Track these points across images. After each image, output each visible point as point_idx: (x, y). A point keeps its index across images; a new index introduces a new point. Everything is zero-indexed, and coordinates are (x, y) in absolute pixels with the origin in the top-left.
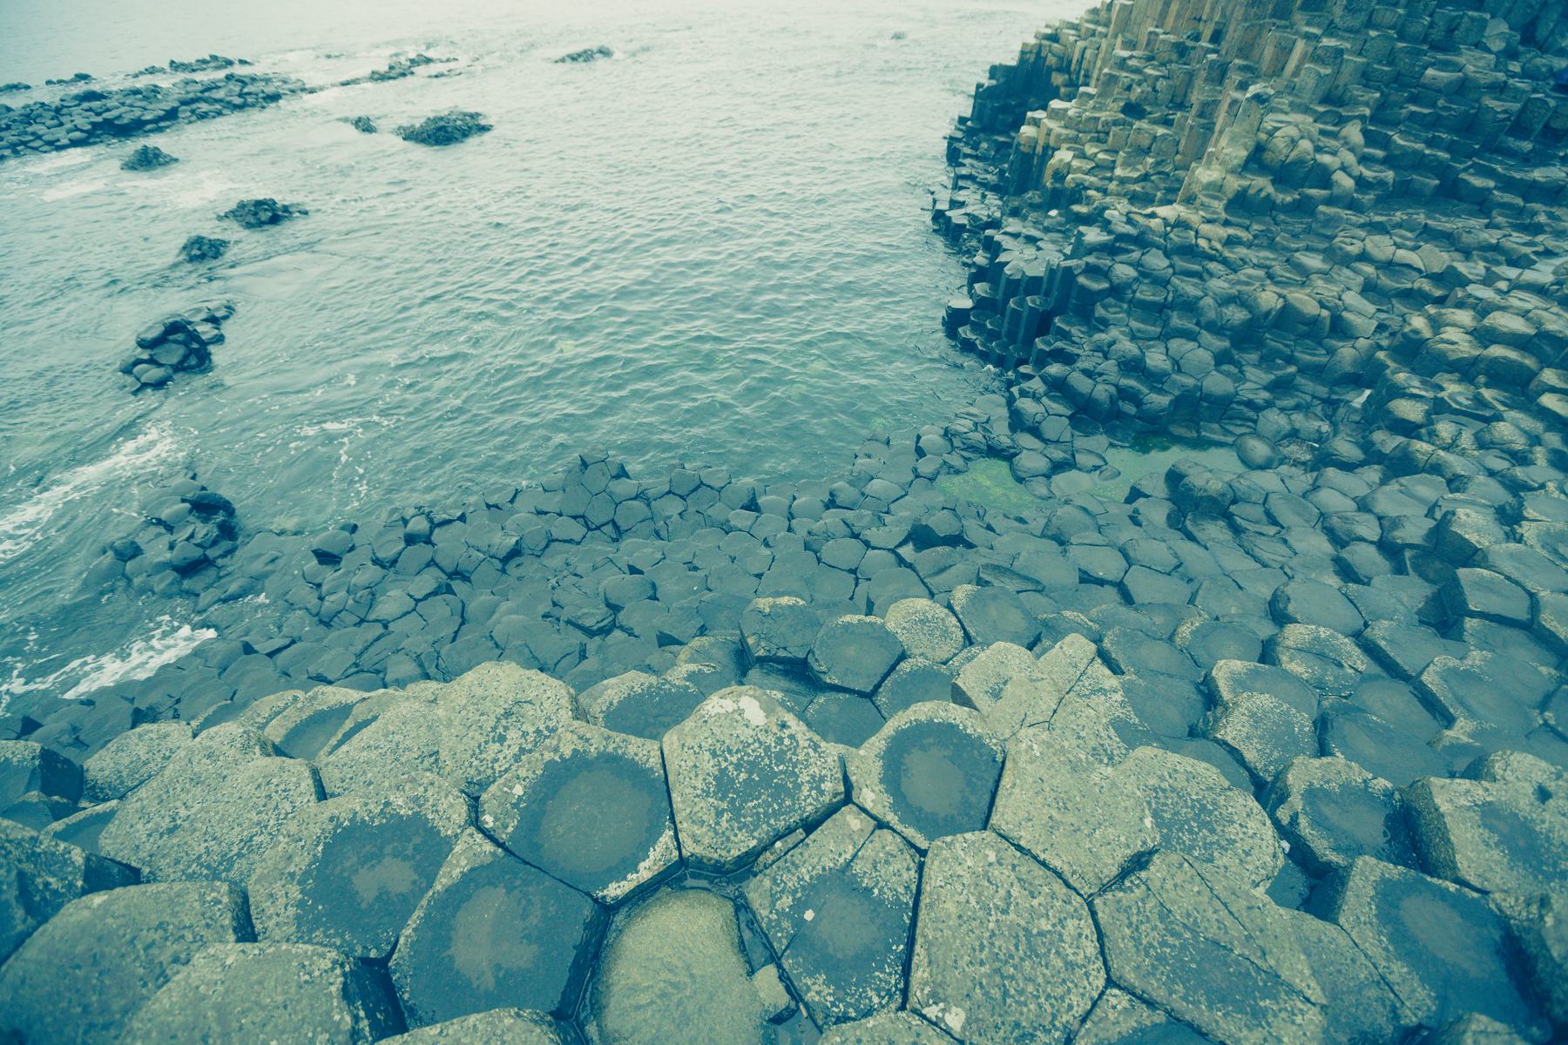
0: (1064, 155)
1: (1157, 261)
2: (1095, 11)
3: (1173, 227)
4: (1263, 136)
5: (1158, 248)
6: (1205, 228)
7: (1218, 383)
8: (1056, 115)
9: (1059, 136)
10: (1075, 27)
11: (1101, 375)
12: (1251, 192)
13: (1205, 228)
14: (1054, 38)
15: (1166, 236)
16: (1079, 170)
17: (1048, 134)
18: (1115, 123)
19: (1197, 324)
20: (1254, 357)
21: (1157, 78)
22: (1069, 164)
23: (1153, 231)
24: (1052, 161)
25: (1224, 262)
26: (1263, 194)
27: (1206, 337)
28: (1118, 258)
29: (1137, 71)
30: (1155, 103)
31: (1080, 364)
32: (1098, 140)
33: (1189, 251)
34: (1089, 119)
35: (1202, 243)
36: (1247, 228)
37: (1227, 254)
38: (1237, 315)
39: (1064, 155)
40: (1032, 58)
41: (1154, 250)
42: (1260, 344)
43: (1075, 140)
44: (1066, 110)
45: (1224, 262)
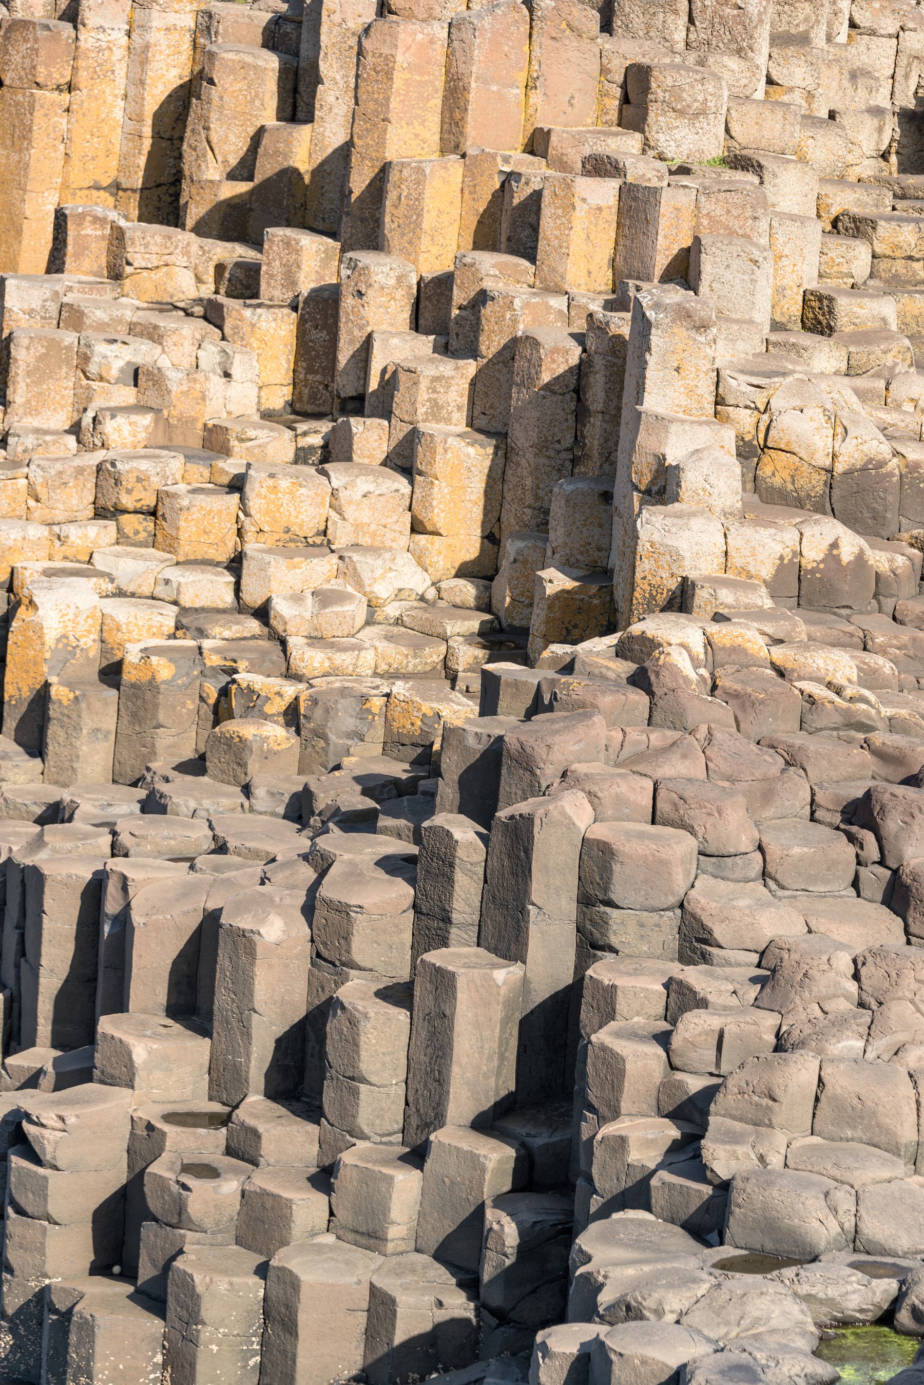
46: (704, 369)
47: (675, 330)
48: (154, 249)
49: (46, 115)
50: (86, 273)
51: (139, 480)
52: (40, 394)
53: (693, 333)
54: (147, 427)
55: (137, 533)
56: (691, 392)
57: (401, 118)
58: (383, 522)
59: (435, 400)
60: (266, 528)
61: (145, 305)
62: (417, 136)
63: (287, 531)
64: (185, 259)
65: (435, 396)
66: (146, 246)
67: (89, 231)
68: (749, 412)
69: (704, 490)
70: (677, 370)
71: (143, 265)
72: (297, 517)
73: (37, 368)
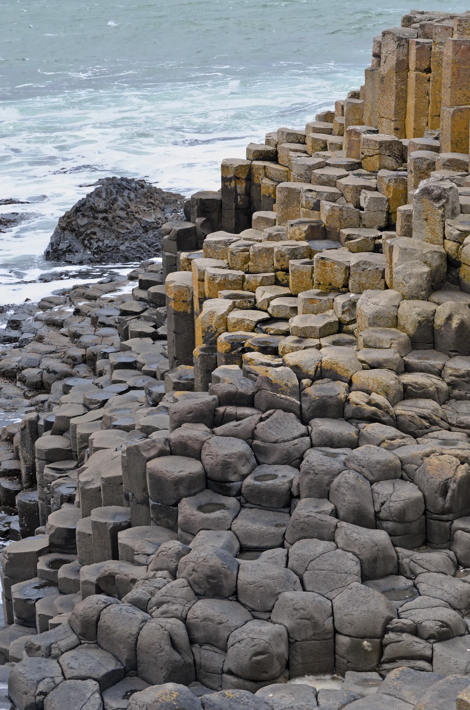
0: (218, 305)
1: (284, 429)
2: (328, 117)
3: (314, 379)
4: (450, 245)
5: (286, 410)
6: (362, 377)
7: (360, 604)
8: (216, 252)
9: (213, 277)
10: (300, 139)
11: (159, 604)
12: (439, 321)
13: (362, 377)
14: (273, 157)
15: (300, 392)
16: (239, 323)
17: (202, 280)
18: (294, 254)
19: (335, 513)
20: (437, 557)
21: (358, 190)
22: (224, 318)
23: (274, 387)
24: (202, 315)
25: (396, 422)
26: (455, 323)
27: (349, 531)
28: (217, 430)
29: (330, 182)
30: (360, 223)
31: (136, 592)
32: (277, 282)
33: (337, 410)
34: (261, 251)
35: (357, 397)
36: (439, 374)
37: (399, 410)
38: (402, 494)
39: (218, 305)
40: (241, 187)
41: (279, 413)
42: (448, 541)
43: (241, 283)
44: (227, 243)
45: (396, 422)
46: (438, 220)
47: (424, 200)
48: (372, 147)
49: (420, 83)
50: (353, 158)
51: (282, 256)
52: (287, 213)
53: (431, 202)
54: (305, 232)
55: (283, 280)
56: (433, 231)
57: (456, 86)
58: (372, 283)
59: (409, 226)
60: (322, 283)
61: (369, 173)
62: (465, 95)
63: (330, 284)
64: (388, 151)
65: (409, 223)
66: (368, 145)
67: (354, 138)
68: (455, 243)
69: (402, 283)
70: (426, 220)
71: (368, 154)
72: (334, 278)
73: (285, 201)
